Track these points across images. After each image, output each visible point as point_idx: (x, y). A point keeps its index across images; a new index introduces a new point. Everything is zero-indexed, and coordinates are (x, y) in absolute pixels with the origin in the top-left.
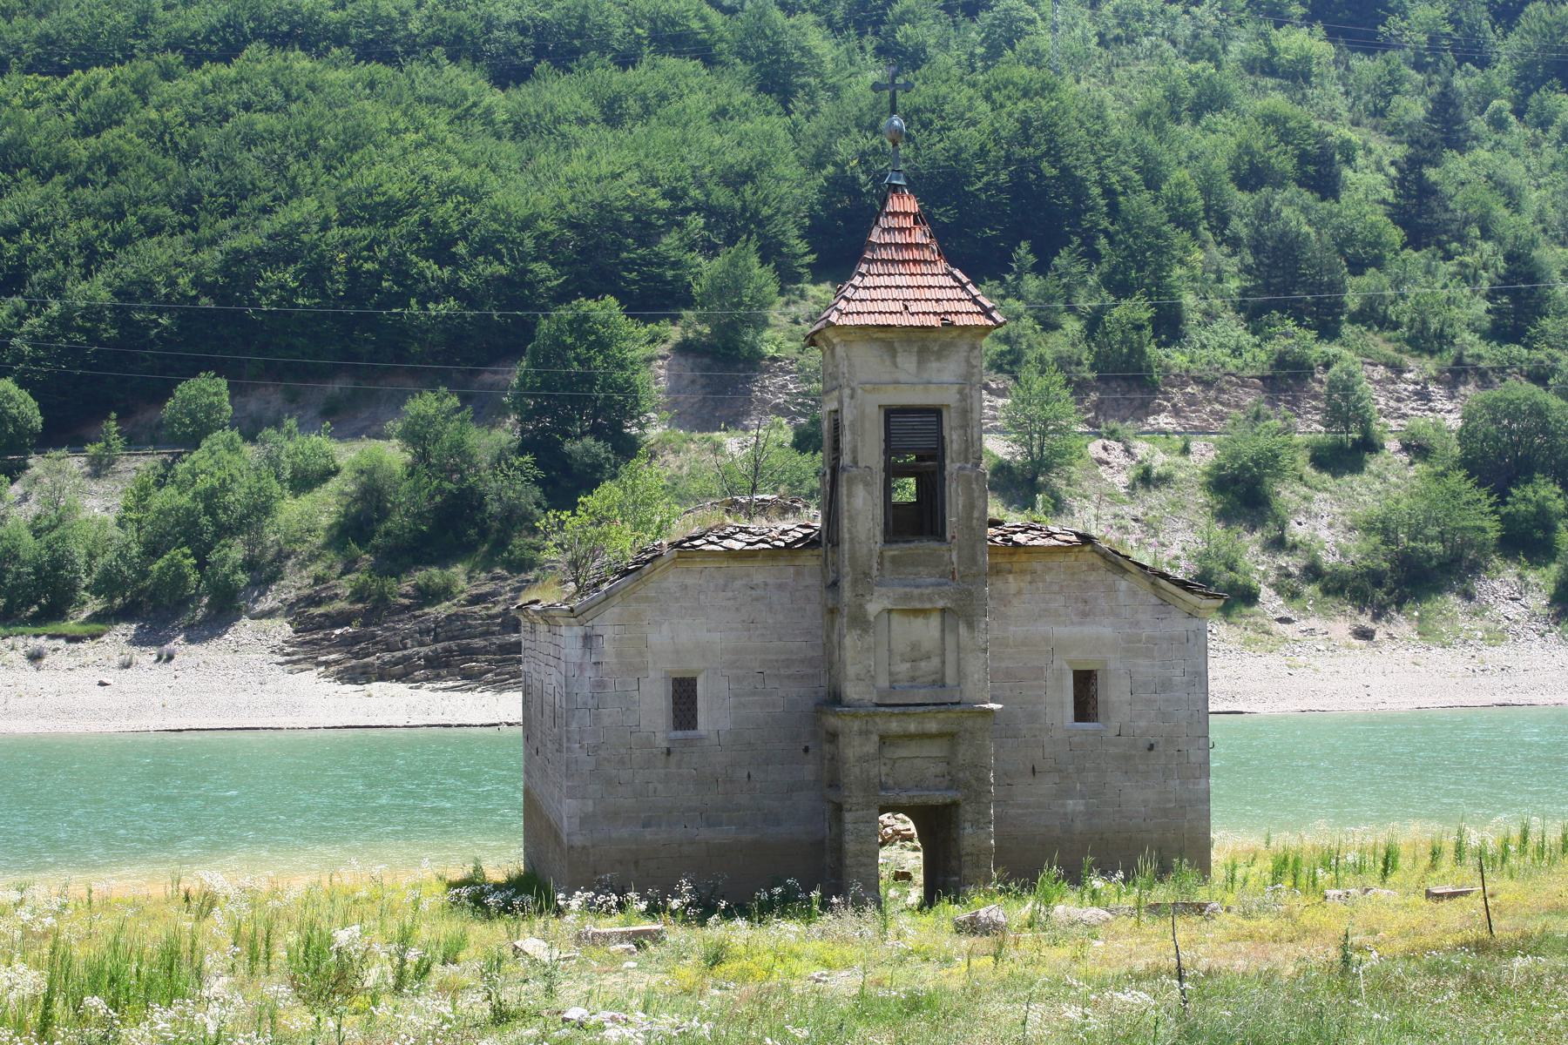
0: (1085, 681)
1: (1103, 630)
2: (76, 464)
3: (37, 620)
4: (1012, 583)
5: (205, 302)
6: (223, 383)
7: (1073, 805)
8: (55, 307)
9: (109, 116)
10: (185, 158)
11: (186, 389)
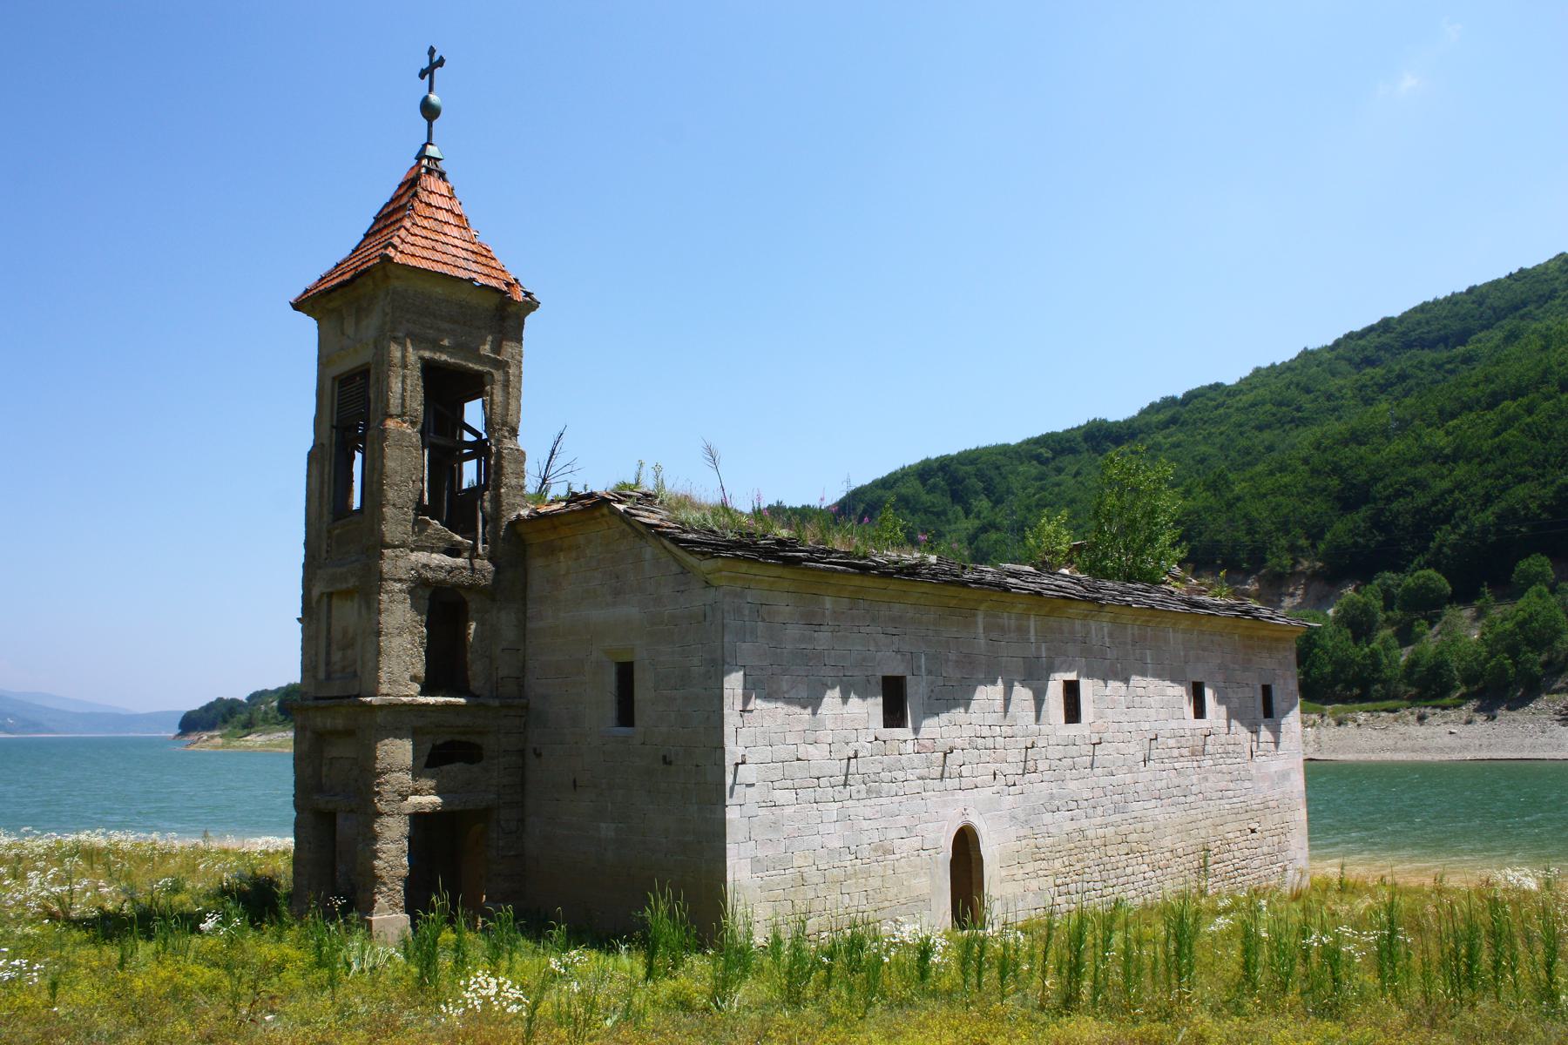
0: (625, 673)
1: (630, 611)
2: (1468, 612)
3: (1427, 700)
4: (564, 562)
5: (1544, 516)
6: (1544, 559)
7: (607, 830)
8: (1464, 528)
9: (1509, 421)
10: (1545, 440)
11: (1522, 565)
